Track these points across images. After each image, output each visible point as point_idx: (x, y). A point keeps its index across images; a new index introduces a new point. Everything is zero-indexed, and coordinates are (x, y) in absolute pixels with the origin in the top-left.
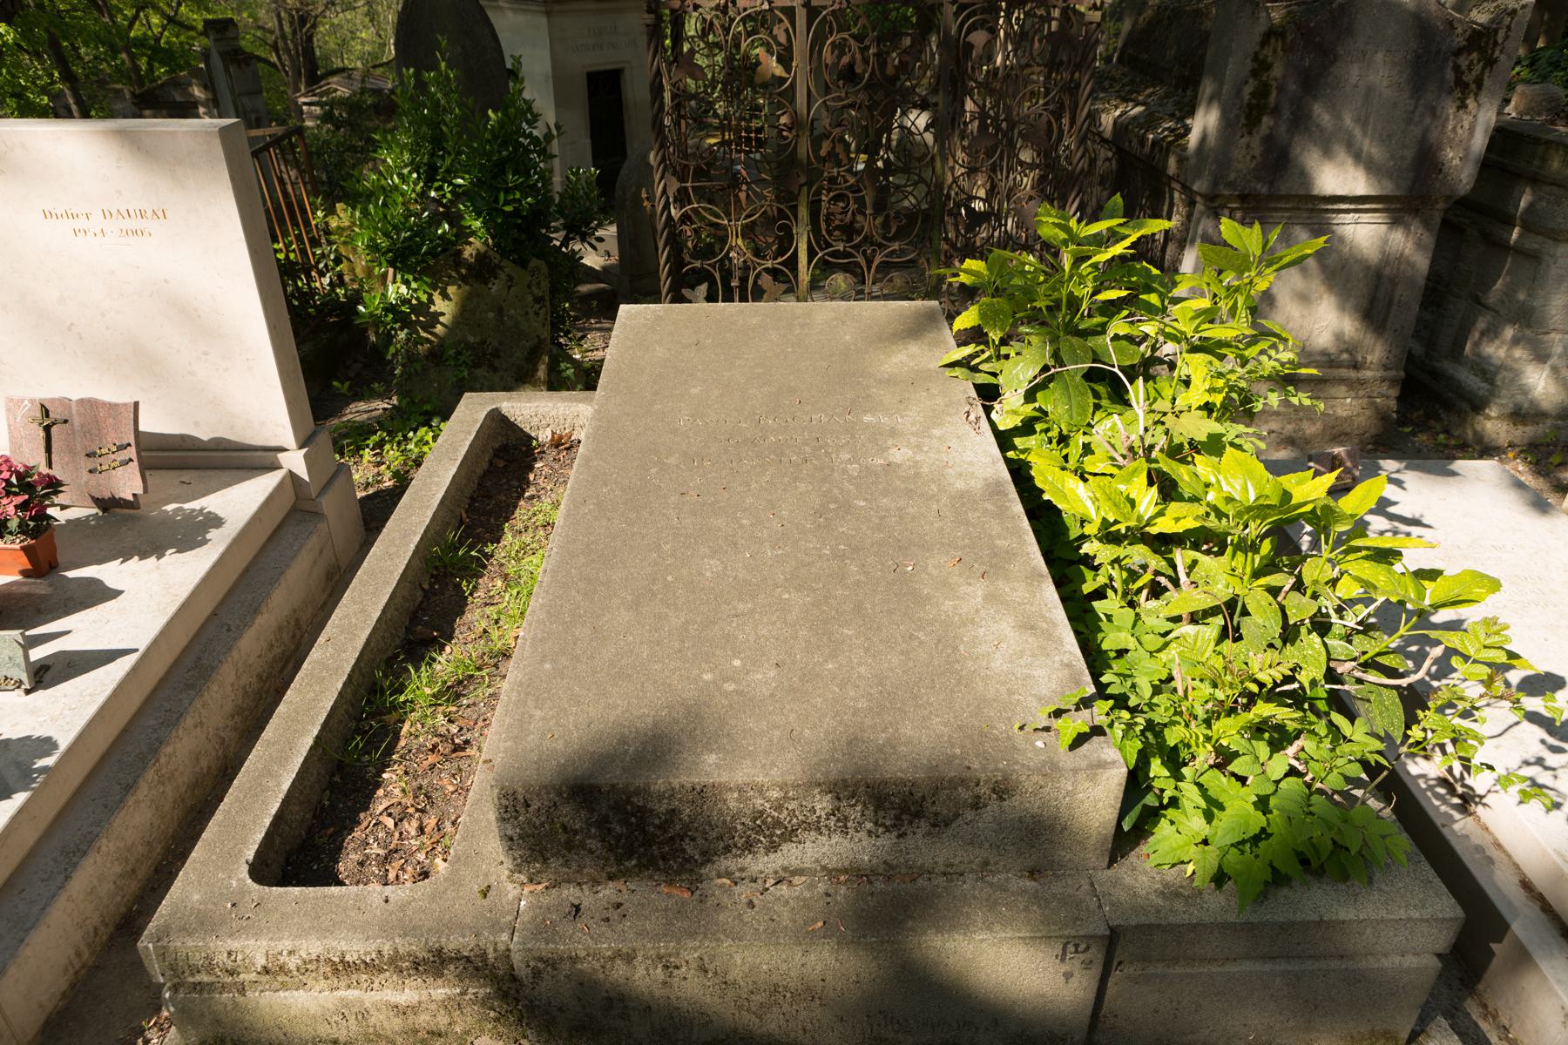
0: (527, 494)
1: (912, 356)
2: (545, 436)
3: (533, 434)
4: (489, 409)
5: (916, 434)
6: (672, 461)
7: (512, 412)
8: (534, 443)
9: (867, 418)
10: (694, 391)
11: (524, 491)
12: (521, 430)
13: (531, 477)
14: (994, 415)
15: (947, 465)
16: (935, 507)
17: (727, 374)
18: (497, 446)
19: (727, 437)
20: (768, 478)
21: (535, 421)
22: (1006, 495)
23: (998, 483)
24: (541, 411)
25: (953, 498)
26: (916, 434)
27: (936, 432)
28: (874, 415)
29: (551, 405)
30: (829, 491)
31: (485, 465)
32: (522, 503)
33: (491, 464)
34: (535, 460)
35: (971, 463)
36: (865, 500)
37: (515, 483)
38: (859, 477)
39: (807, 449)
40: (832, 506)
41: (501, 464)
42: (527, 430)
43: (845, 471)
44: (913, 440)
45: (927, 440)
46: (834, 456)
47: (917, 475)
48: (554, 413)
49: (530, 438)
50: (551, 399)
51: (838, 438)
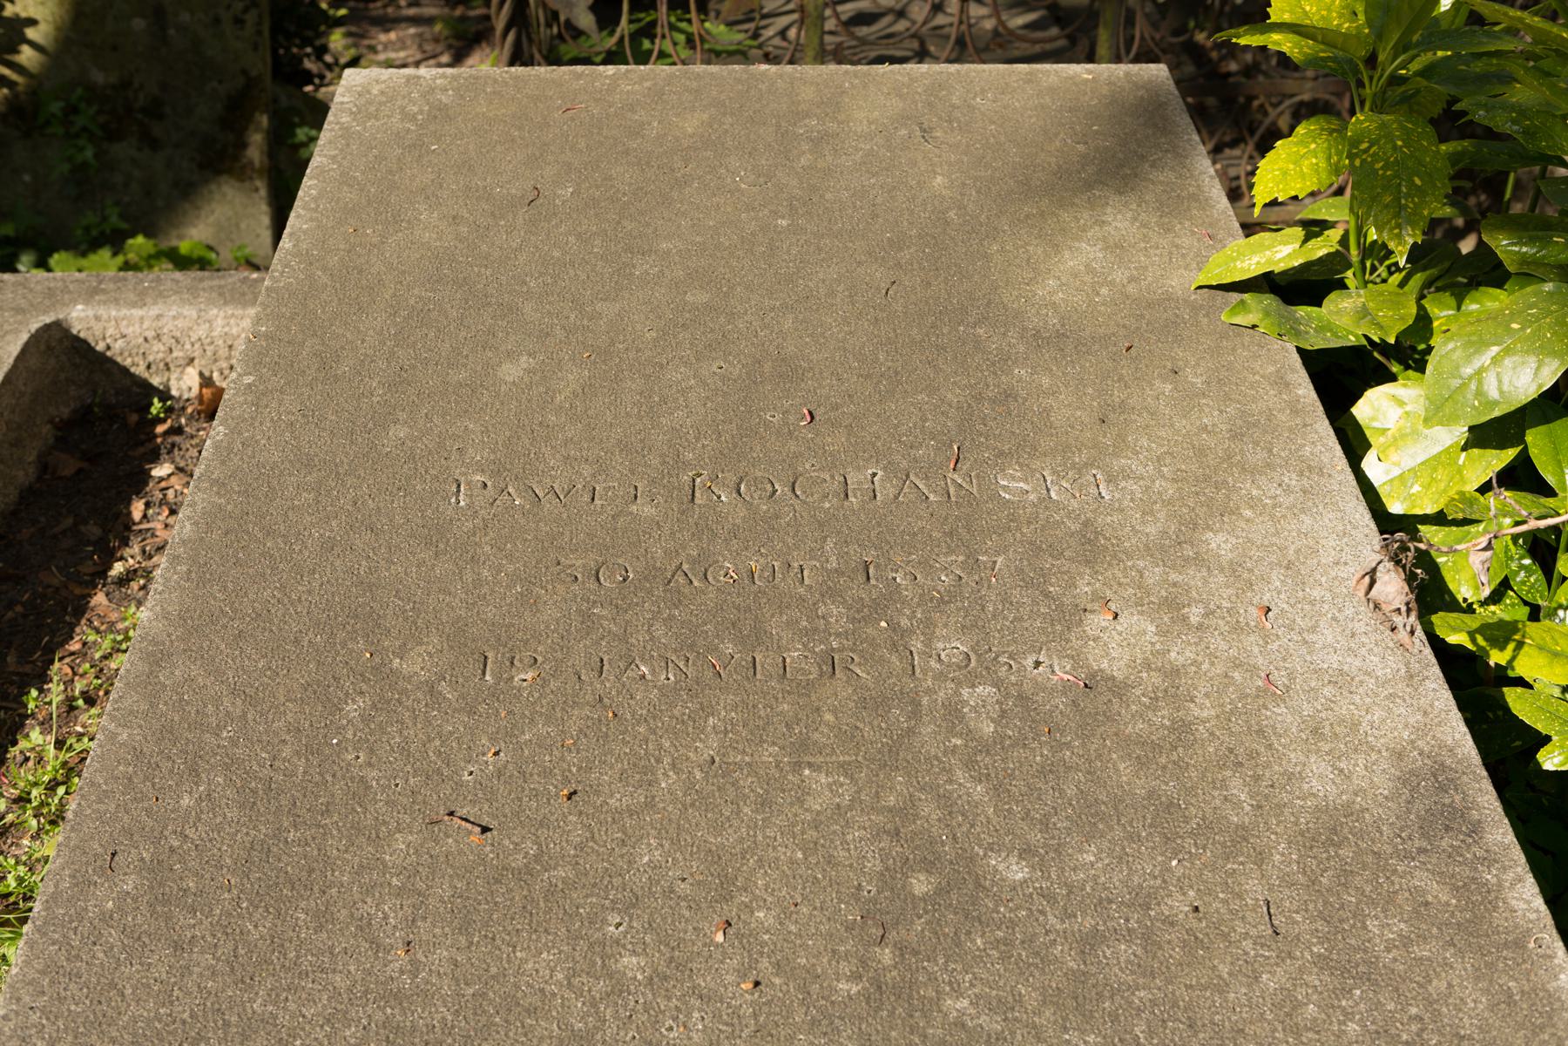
0: (118, 568)
1: (1116, 248)
2: (186, 384)
3: (156, 381)
4: (34, 326)
5: (1159, 551)
6: (414, 665)
7: (97, 328)
8: (157, 405)
9: (1012, 484)
10: (511, 372)
11: (110, 557)
12: (125, 371)
13: (137, 508)
14: (1370, 465)
15: (1269, 691)
16: (1254, 888)
17: (608, 309)
18: (65, 412)
19: (592, 559)
20: (709, 747)
21: (157, 351)
22: (1475, 830)
23: (1441, 776)
24: (168, 326)
25: (1307, 841)
26: (1159, 551)
27: (1219, 543)
28: (1028, 472)
29: (190, 312)
30: (906, 811)
31: (24, 475)
32: (99, 599)
33: (44, 467)
34: (155, 457)
35: (1342, 680)
36: (1026, 853)
37: (93, 530)
38: (999, 738)
39: (835, 611)
40: (921, 885)
41: (68, 466)
42: (139, 370)
43: (953, 713)
44: (1154, 575)
45: (1193, 577)
46: (917, 645)
47: (1182, 729)
48: (201, 331)
49: (147, 391)
50: (193, 292)
51: (924, 564)
